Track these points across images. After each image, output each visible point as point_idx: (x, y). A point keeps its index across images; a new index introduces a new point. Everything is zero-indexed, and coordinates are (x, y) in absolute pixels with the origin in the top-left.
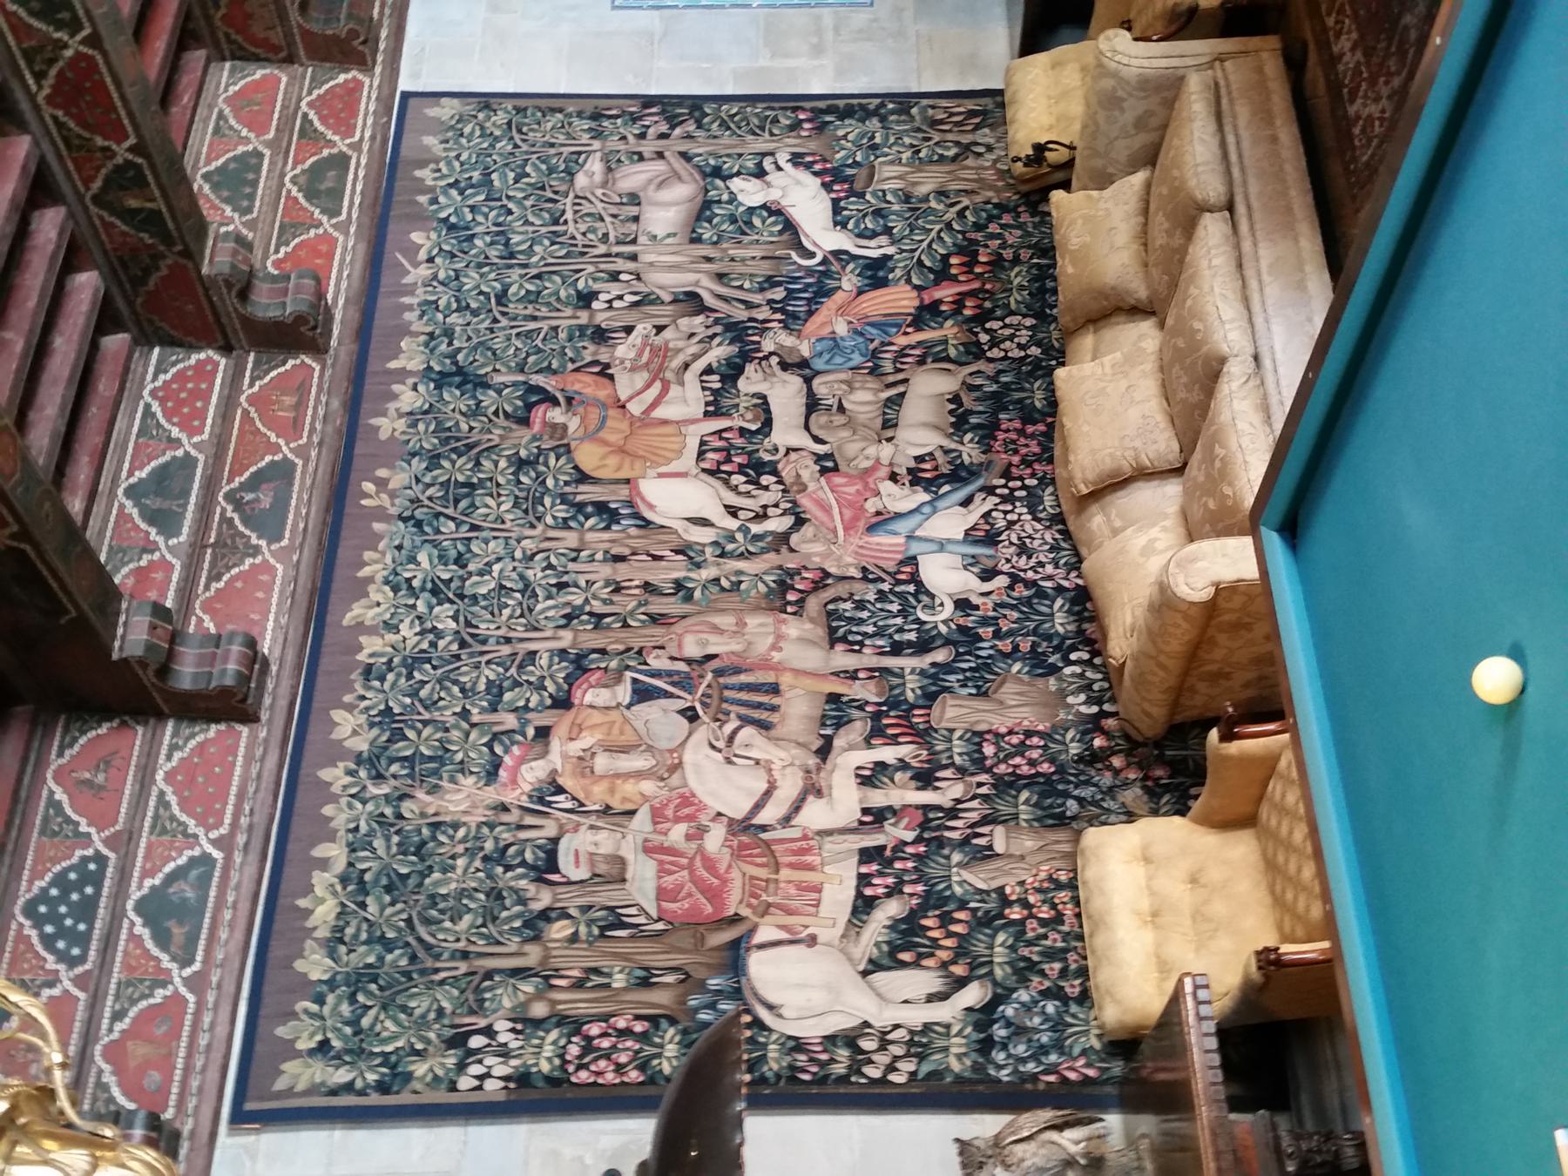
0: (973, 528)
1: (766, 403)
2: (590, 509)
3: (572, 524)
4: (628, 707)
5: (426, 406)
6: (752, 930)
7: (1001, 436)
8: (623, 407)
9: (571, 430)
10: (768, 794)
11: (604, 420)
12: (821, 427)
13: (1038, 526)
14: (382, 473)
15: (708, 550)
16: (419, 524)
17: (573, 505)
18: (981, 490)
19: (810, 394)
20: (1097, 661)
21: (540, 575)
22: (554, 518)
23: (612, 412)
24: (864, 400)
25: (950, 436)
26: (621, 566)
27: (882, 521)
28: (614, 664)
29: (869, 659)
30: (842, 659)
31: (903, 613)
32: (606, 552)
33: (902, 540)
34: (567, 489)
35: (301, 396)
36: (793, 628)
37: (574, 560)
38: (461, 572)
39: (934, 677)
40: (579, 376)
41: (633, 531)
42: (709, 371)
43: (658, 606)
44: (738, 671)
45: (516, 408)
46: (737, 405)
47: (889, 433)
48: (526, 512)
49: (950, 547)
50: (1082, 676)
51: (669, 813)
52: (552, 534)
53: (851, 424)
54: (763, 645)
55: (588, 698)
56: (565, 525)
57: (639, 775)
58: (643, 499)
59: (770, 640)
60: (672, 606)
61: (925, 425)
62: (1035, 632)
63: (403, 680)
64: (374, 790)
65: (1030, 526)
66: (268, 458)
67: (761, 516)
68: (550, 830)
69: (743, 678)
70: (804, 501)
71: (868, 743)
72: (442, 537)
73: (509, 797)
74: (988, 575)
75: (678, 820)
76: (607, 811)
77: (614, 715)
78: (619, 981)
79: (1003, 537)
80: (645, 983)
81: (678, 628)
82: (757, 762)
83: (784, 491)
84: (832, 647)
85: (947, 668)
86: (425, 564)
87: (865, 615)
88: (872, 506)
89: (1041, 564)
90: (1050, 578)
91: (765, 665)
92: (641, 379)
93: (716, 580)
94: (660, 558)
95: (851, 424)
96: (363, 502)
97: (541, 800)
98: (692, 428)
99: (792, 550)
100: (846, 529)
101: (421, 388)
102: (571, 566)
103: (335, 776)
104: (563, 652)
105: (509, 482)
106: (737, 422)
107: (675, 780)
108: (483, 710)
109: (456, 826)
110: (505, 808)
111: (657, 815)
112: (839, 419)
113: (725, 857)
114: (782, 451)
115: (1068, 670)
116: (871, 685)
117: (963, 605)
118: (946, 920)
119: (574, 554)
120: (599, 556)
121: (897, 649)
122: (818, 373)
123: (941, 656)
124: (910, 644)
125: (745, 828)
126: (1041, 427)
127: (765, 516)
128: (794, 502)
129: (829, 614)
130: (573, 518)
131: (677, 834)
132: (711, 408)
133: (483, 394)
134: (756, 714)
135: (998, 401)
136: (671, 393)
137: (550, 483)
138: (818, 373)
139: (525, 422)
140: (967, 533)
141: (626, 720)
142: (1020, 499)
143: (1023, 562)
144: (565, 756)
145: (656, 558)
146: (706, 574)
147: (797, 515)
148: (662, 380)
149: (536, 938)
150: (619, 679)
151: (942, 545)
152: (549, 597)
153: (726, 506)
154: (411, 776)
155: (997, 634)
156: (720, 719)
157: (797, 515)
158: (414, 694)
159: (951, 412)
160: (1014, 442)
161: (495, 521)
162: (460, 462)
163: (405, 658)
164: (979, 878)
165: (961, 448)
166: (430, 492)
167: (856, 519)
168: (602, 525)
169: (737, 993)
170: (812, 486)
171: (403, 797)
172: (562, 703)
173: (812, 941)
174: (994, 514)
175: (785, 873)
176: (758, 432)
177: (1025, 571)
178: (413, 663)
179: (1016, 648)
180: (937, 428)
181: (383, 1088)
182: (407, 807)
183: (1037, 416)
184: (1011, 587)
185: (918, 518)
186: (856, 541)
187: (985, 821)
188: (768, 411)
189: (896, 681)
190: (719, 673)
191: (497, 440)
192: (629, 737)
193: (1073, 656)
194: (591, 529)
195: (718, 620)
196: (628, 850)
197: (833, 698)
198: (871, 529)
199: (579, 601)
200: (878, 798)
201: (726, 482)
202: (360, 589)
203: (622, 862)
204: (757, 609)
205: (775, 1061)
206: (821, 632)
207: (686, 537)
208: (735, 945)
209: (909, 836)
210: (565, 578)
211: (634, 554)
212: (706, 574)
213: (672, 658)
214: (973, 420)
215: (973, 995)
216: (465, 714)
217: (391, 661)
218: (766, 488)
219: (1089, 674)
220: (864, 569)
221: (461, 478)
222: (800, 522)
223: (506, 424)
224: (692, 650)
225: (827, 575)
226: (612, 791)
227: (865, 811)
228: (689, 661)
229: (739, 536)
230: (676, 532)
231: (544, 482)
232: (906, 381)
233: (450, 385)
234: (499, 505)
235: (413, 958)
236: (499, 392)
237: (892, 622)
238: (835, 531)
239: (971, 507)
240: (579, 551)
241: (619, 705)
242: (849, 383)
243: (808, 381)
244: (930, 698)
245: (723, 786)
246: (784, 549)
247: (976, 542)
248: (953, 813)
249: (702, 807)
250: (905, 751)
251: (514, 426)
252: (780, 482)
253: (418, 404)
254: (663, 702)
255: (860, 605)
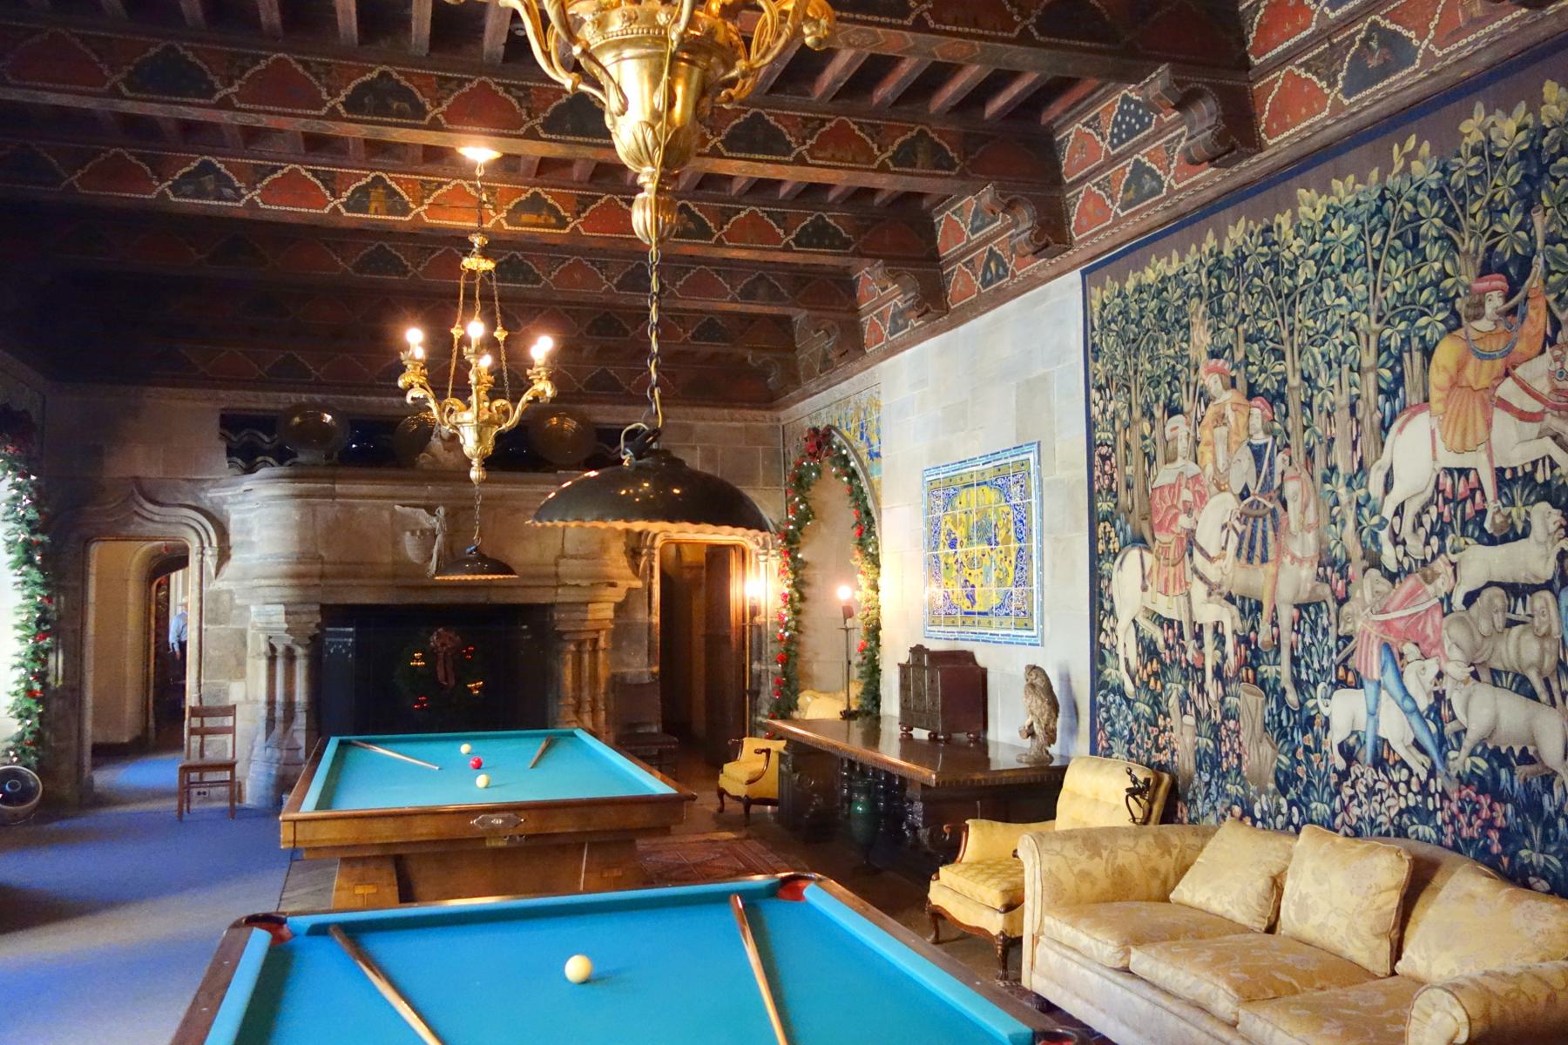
0: (1389, 747)
1: (1517, 538)
2: (1398, 369)
3: (1384, 356)
4: (1250, 445)
5: (1499, 154)
6: (1149, 549)
7: (1485, 801)
8: (1507, 374)
9: (1478, 325)
10: (1208, 557)
11: (1491, 358)
12: (1490, 600)
13: (1393, 812)
14: (1426, 147)
15: (1362, 492)
16: (1379, 210)
17: (1401, 352)
18: (1433, 764)
19: (1534, 589)
20: (1291, 828)
21: (1337, 342)
22: (1389, 338)
23: (1499, 364)
24: (1523, 651)
25: (1483, 742)
26: (1347, 411)
27: (1397, 660)
28: (1277, 426)
29: (1287, 637)
30: (1287, 614)
31: (1322, 671)
32: (1358, 397)
33: (1376, 676)
34: (1415, 342)
35: (1487, 17)
36: (1307, 573)
37: (1351, 369)
38: (1338, 270)
39: (1274, 690)
40: (1543, 311)
41: (1378, 415)
42: (1554, 466)
43: (1319, 452)
44: (1275, 529)
45: (1502, 254)
46: (1512, 503)
47: (1485, 676)
48: (1395, 307)
49: (1371, 723)
50: (1279, 812)
51: (1197, 488)
52: (1373, 339)
53: (1495, 634)
54: (1296, 548)
55: (1256, 411)
56: (1383, 348)
57: (1215, 462)
58: (1408, 420)
59: (1299, 554)
60: (1319, 468)
61: (1496, 718)
62: (1310, 782)
63: (1263, 260)
64: (1204, 272)
65: (1395, 804)
66: (1412, 34)
67: (1396, 540)
68: (1187, 406)
69: (1270, 533)
70: (1409, 583)
71: (1234, 632)
72: (1367, 238)
73: (1202, 371)
74: (1348, 753)
75: (1194, 493)
76: (1197, 443)
77: (1243, 434)
78: (1129, 470)
79: (1382, 776)
80: (1129, 487)
81: (1305, 475)
82: (1224, 549)
83: (1424, 562)
84: (1297, 606)
85: (1282, 701)
86: (1345, 234)
87: (1320, 636)
88: (1409, 649)
89: (1360, 805)
90: (1345, 808)
91: (1280, 551)
92: (1542, 386)
93: (1337, 503)
94: (1354, 448)
95: (1495, 634)
96: (1396, 147)
97: (1201, 395)
98: (1484, 457)
99: (1365, 571)
100: (1386, 623)
101: (1522, 135)
102: (1346, 367)
103: (1210, 242)
104: (1285, 381)
105: (1423, 279)
106: (1492, 506)
107: (1214, 489)
108: (1246, 331)
109: (1187, 341)
110: (1196, 370)
111: (1196, 478)
112: (1499, 621)
113: (1178, 530)
114: (1454, 558)
115: (1283, 801)
116: (1268, 638)
117: (1327, 725)
118: (1155, 674)
119: (1355, 367)
120: (1355, 391)
121: (1295, 661)
122: (1557, 597)
123: (1292, 697)
124: (1299, 672)
125: (1190, 542)
126: (1496, 848)
127: (1396, 544)
128: (1410, 571)
129: (1318, 605)
130: (1390, 356)
131: (1187, 495)
132: (1508, 475)
133: (1517, 211)
134: (1245, 545)
135: (1530, 806)
136: (1527, 426)
137: (1423, 321)
138: (1557, 597)
139: (1485, 270)
140: (1385, 740)
141: (1240, 444)
142: (1425, 802)
143: (1361, 788)
144: (1223, 405)
145: (1354, 444)
146: (1342, 491)
147: (1397, 575)
148: (1543, 412)
149: (1144, 414)
150: (1267, 432)
151: (1373, 714)
152: (1323, 356)
153: (1403, 504)
154: (1211, 296)
155: (1307, 749)
156: (1244, 517)
157: (1397, 575)
158: (1255, 274)
159: (1511, 749)
160: (1475, 812)
161: (1383, 281)
162: (1437, 221)
163: (1278, 254)
164: (1174, 702)
165: (1464, 752)
166: (1409, 206)
167: (1398, 633)
168: (1383, 385)
169: (1126, 544)
170: (1430, 588)
171: (1200, 296)
172: (1252, 392)
173: (1144, 589)
174: (1405, 772)
175: (1172, 570)
176: (1483, 530)
177: (1353, 787)
178: (1274, 263)
179: (1299, 762)
180: (1493, 731)
181: (1094, 345)
182: (1196, 300)
183: (1511, 847)
184: (1335, 771)
185: (1399, 695)
186: (1374, 631)
187: (1198, 712)
188: (1505, 540)
189: (1271, 656)
190: (1273, 512)
191: (1462, 248)
192: (1234, 447)
193: (1295, 809)
194: (1379, 376)
195: (1311, 507)
196: (1180, 462)
197: (1259, 606)
198: (1387, 647)
199: (1320, 383)
200: (1208, 636)
201: (1431, 501)
202: (1325, 189)
203: (1174, 460)
204: (1321, 541)
205: (1106, 566)
206: (1303, 597)
207: (1374, 469)
208: (1143, 540)
209: (1189, 657)
210: (1335, 365)
211: (1358, 422)
212: (1342, 491)
213: (1283, 474)
214: (1504, 773)
215: (1129, 688)
216: (1243, 318)
217: (1275, 243)
218: (1427, 543)
219: (1280, 818)
220: (1349, 638)
221: (1423, 230)
222: (1392, 577)
223: (1481, 250)
224: (1291, 488)
225: (1341, 602)
226: (1208, 444)
227: (1201, 626)
228: (1281, 488)
229: (1376, 520)
230: (1378, 458)
231: (1423, 314)
232: (1553, 704)
233: (1527, 167)
234: (1398, 279)
235: (1134, 341)
236: (1520, 227)
237: (1315, 659)
238: (1384, 611)
239: (1414, 750)
240: (1359, 371)
241: (1250, 436)
242: (1547, 635)
243: (1548, 586)
244: (1262, 683)
245: (1214, 521)
246: (1366, 563)
247: (1375, 747)
248: (1201, 689)
249: (1201, 509)
250: (1232, 661)
251: (1479, 261)
252: (1434, 557)
253: (1503, 143)
254: (1254, 470)
255: (1325, 632)
